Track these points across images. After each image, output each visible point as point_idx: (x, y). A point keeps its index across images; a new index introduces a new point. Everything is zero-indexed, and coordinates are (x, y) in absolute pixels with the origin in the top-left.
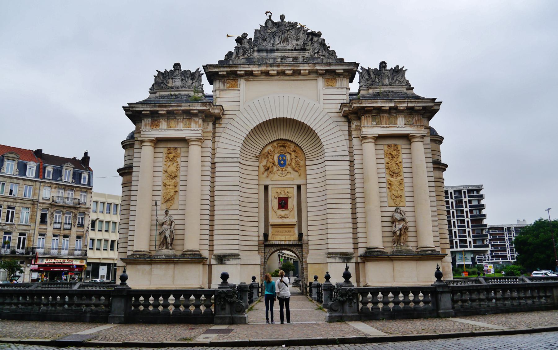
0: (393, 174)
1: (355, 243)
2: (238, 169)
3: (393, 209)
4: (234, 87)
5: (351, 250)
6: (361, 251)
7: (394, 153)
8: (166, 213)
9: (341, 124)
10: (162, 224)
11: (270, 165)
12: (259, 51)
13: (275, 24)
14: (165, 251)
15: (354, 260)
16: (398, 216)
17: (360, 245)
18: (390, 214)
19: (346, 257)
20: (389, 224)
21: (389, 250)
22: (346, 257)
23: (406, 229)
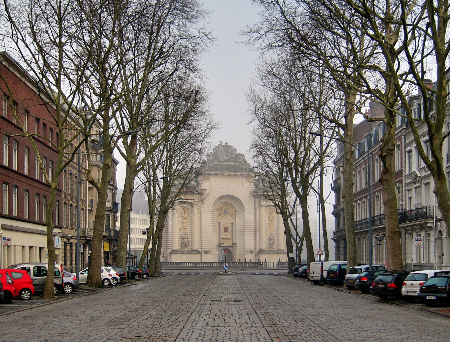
0: (271, 220)
1: (255, 247)
2: (211, 216)
3: (270, 234)
4: (208, 179)
5: (253, 250)
6: (257, 250)
7: (272, 212)
8: (185, 234)
9: (252, 198)
10: (184, 238)
11: (221, 213)
12: (217, 161)
13: (223, 146)
14: (186, 249)
15: (254, 253)
16: (272, 237)
17: (257, 248)
18: (268, 236)
19: (251, 252)
20: (268, 240)
21: (267, 250)
22: (251, 252)
23: (274, 242)
